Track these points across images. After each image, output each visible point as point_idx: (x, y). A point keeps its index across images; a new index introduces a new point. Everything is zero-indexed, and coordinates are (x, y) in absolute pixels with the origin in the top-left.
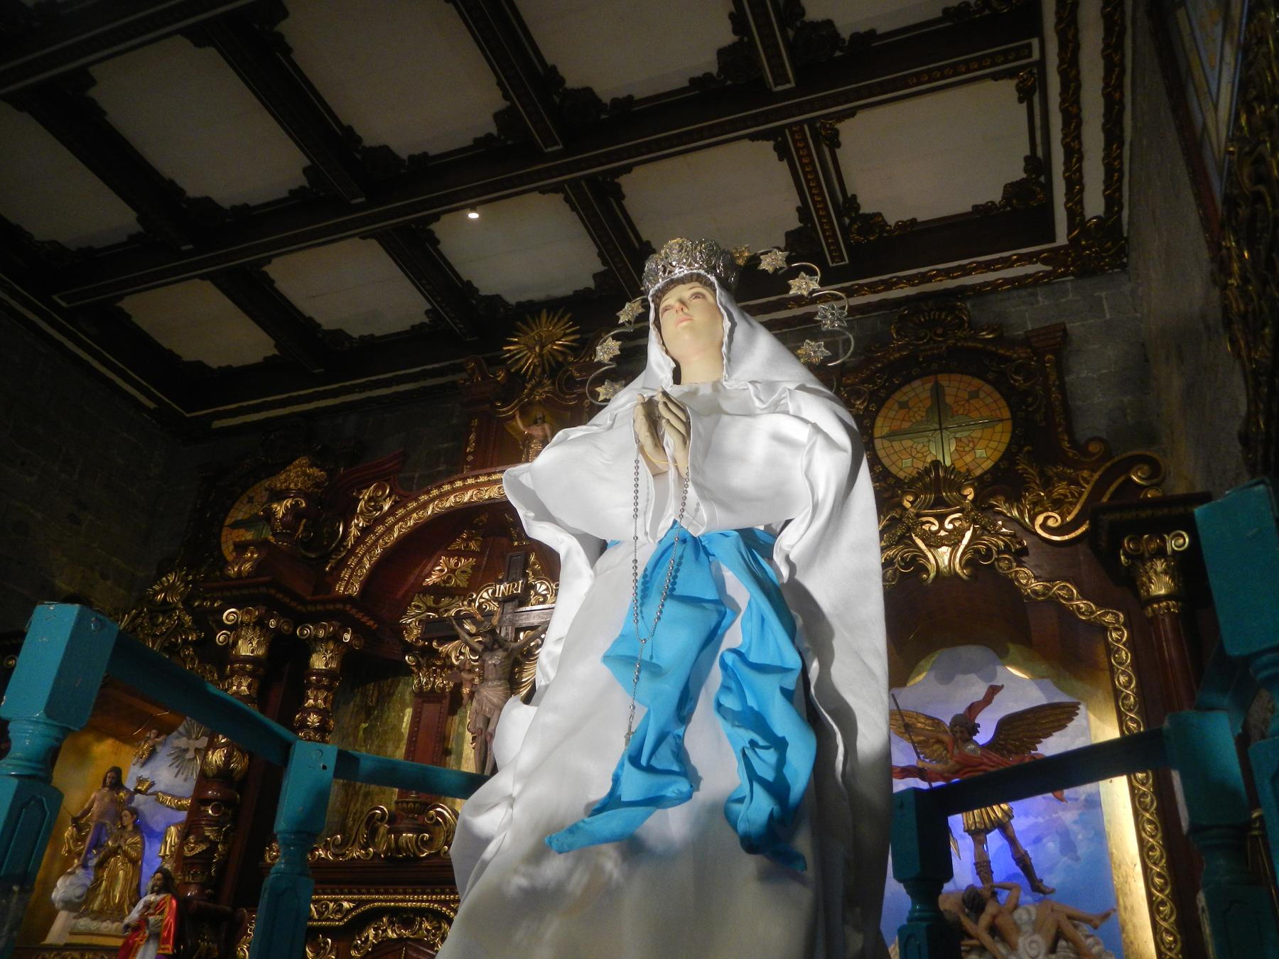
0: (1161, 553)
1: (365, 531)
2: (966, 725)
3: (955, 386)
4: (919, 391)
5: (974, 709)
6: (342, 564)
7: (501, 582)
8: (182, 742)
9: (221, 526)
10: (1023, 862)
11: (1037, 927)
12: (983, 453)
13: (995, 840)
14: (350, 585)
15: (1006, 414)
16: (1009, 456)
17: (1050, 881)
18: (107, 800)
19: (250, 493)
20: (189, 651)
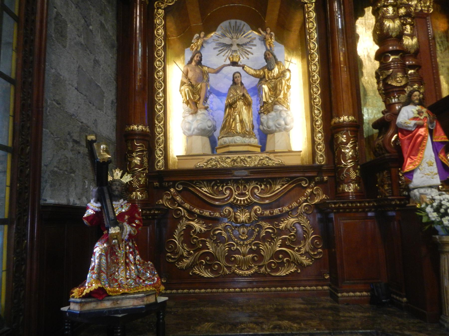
18: (198, 71)
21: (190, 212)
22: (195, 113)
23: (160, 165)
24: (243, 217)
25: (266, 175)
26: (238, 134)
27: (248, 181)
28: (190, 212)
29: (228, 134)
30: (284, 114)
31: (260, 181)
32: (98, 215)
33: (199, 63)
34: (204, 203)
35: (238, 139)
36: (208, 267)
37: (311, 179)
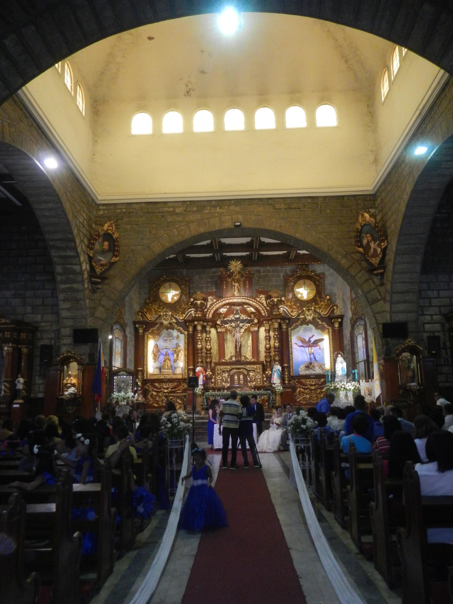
0: (337, 321)
1: (211, 305)
2: (309, 341)
3: (307, 281)
4: (301, 281)
5: (310, 338)
6: (207, 311)
7: (235, 314)
8: (166, 338)
9: (158, 292)
10: (315, 358)
11: (317, 366)
12: (312, 296)
13: (312, 355)
14: (210, 315)
15: (315, 288)
16: (315, 296)
17: (317, 359)
19: (164, 285)
20: (174, 324)
21: (153, 390)
22: (155, 362)
23: (145, 378)
24: (166, 391)
25: (171, 381)
26: (166, 369)
27: (167, 382)
28: (153, 390)
29: (164, 369)
30: (179, 363)
31: (171, 382)
32: (136, 390)
33: (157, 347)
34: (156, 387)
35: (166, 371)
36: (157, 403)
37: (183, 382)
